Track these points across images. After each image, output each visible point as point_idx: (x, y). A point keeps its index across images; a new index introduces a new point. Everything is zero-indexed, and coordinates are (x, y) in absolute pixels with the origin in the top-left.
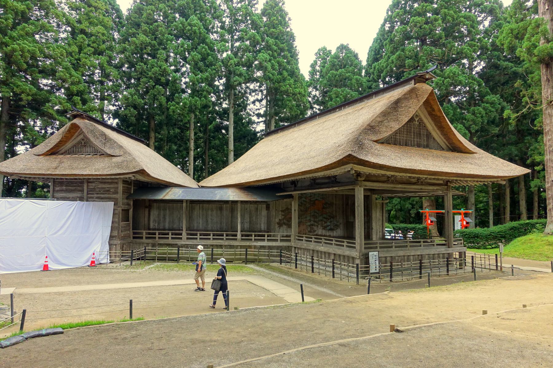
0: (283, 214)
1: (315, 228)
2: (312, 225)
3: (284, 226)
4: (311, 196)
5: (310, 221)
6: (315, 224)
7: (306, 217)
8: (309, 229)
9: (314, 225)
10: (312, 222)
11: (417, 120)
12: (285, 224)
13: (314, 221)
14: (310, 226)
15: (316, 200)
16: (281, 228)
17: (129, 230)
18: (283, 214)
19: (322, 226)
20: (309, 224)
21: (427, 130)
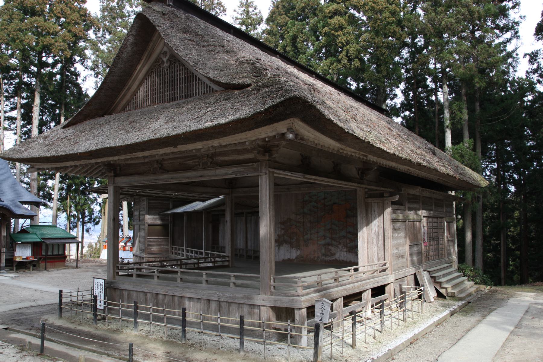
0: (283, 227)
1: (333, 249)
2: (329, 244)
3: (284, 245)
4: (324, 199)
5: (325, 237)
6: (334, 243)
7: (318, 232)
8: (323, 251)
9: (332, 245)
10: (328, 240)
11: (165, 59)
12: (286, 242)
13: (332, 239)
14: (324, 245)
15: (334, 203)
16: (282, 248)
17: (167, 245)
18: (283, 227)
19: (347, 247)
20: (323, 242)
21: (186, 69)
